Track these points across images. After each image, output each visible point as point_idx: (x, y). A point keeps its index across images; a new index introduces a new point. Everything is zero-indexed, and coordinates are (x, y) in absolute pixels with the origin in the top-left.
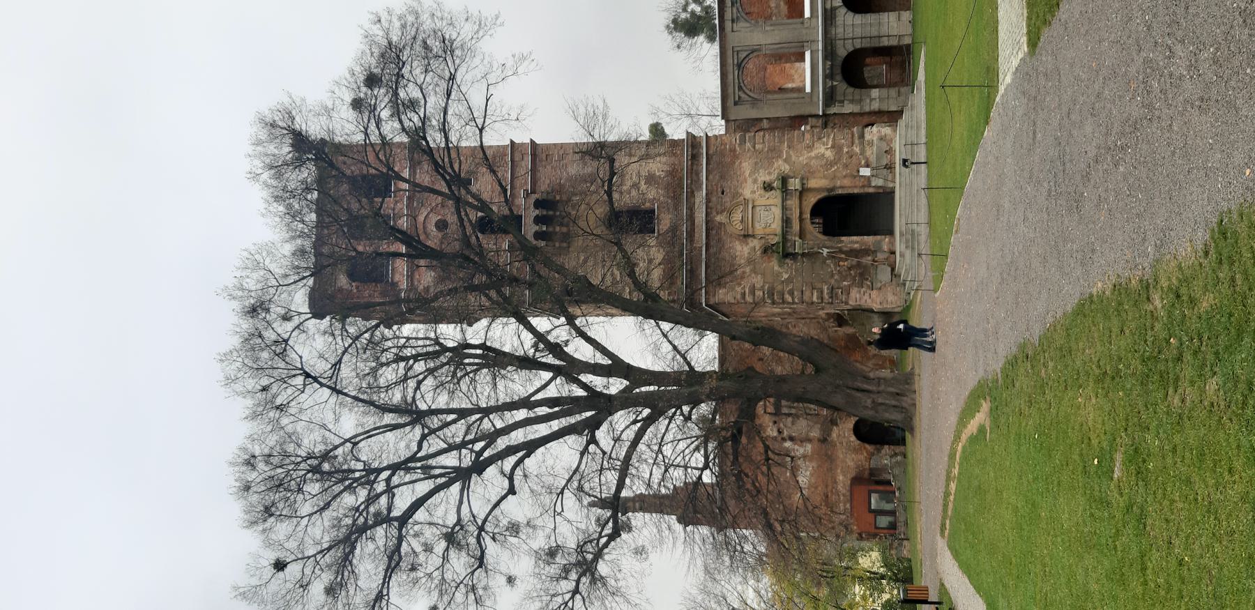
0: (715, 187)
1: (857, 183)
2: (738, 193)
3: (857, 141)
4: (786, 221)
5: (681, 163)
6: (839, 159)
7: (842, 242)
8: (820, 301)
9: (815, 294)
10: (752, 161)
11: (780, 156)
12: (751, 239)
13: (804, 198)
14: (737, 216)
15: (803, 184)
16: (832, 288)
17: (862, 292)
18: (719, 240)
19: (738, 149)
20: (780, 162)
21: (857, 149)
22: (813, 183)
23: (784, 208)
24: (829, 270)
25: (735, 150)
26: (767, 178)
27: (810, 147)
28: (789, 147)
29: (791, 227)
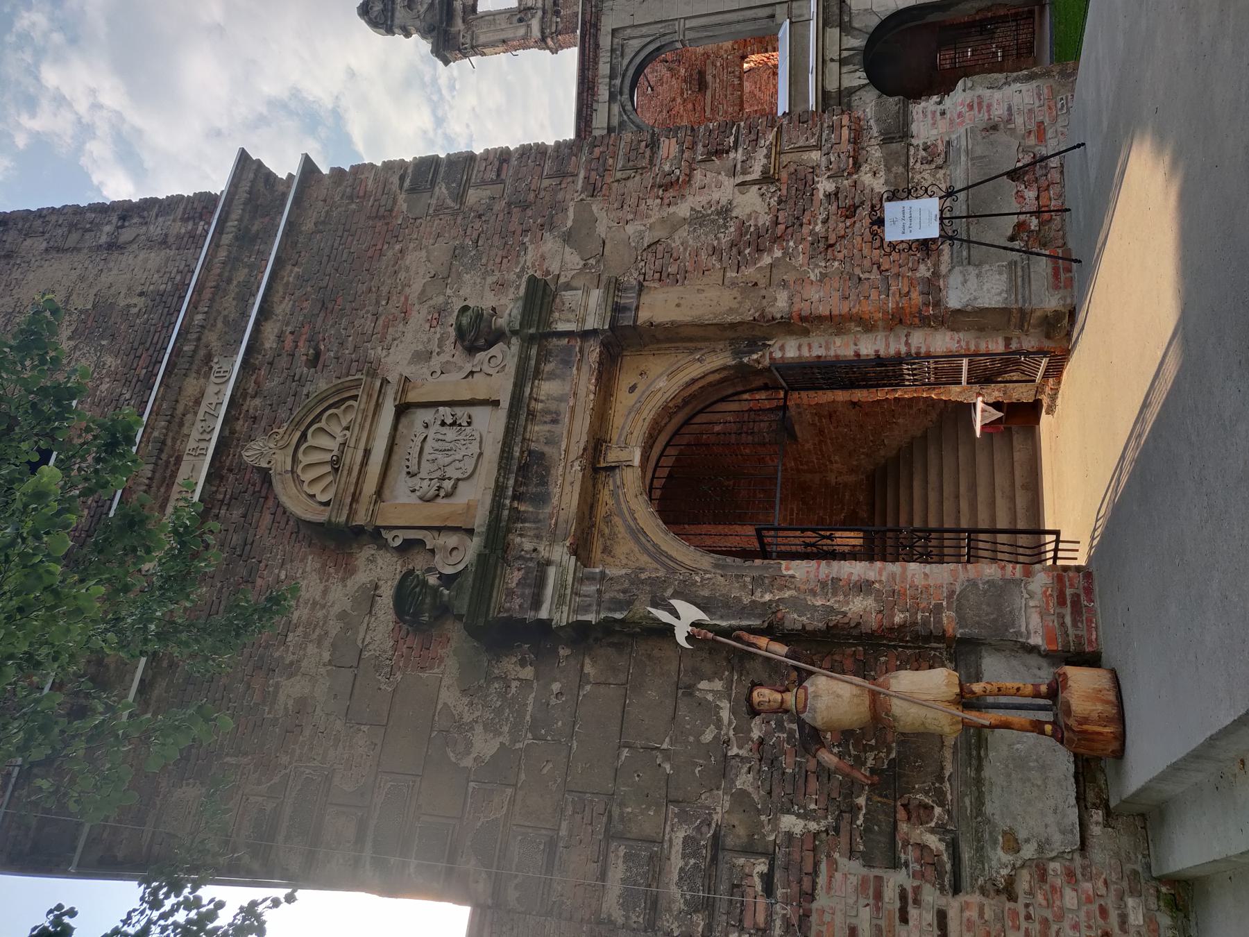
3: (875, 152)
4: (523, 469)
6: (798, 222)
7: (779, 582)
8: (638, 918)
9: (617, 872)
12: (369, 551)
13: (625, 380)
16: (716, 841)
17: (890, 895)
19: (402, 205)
24: (708, 737)
27: (672, 186)
28: (593, 190)
29: (541, 499)
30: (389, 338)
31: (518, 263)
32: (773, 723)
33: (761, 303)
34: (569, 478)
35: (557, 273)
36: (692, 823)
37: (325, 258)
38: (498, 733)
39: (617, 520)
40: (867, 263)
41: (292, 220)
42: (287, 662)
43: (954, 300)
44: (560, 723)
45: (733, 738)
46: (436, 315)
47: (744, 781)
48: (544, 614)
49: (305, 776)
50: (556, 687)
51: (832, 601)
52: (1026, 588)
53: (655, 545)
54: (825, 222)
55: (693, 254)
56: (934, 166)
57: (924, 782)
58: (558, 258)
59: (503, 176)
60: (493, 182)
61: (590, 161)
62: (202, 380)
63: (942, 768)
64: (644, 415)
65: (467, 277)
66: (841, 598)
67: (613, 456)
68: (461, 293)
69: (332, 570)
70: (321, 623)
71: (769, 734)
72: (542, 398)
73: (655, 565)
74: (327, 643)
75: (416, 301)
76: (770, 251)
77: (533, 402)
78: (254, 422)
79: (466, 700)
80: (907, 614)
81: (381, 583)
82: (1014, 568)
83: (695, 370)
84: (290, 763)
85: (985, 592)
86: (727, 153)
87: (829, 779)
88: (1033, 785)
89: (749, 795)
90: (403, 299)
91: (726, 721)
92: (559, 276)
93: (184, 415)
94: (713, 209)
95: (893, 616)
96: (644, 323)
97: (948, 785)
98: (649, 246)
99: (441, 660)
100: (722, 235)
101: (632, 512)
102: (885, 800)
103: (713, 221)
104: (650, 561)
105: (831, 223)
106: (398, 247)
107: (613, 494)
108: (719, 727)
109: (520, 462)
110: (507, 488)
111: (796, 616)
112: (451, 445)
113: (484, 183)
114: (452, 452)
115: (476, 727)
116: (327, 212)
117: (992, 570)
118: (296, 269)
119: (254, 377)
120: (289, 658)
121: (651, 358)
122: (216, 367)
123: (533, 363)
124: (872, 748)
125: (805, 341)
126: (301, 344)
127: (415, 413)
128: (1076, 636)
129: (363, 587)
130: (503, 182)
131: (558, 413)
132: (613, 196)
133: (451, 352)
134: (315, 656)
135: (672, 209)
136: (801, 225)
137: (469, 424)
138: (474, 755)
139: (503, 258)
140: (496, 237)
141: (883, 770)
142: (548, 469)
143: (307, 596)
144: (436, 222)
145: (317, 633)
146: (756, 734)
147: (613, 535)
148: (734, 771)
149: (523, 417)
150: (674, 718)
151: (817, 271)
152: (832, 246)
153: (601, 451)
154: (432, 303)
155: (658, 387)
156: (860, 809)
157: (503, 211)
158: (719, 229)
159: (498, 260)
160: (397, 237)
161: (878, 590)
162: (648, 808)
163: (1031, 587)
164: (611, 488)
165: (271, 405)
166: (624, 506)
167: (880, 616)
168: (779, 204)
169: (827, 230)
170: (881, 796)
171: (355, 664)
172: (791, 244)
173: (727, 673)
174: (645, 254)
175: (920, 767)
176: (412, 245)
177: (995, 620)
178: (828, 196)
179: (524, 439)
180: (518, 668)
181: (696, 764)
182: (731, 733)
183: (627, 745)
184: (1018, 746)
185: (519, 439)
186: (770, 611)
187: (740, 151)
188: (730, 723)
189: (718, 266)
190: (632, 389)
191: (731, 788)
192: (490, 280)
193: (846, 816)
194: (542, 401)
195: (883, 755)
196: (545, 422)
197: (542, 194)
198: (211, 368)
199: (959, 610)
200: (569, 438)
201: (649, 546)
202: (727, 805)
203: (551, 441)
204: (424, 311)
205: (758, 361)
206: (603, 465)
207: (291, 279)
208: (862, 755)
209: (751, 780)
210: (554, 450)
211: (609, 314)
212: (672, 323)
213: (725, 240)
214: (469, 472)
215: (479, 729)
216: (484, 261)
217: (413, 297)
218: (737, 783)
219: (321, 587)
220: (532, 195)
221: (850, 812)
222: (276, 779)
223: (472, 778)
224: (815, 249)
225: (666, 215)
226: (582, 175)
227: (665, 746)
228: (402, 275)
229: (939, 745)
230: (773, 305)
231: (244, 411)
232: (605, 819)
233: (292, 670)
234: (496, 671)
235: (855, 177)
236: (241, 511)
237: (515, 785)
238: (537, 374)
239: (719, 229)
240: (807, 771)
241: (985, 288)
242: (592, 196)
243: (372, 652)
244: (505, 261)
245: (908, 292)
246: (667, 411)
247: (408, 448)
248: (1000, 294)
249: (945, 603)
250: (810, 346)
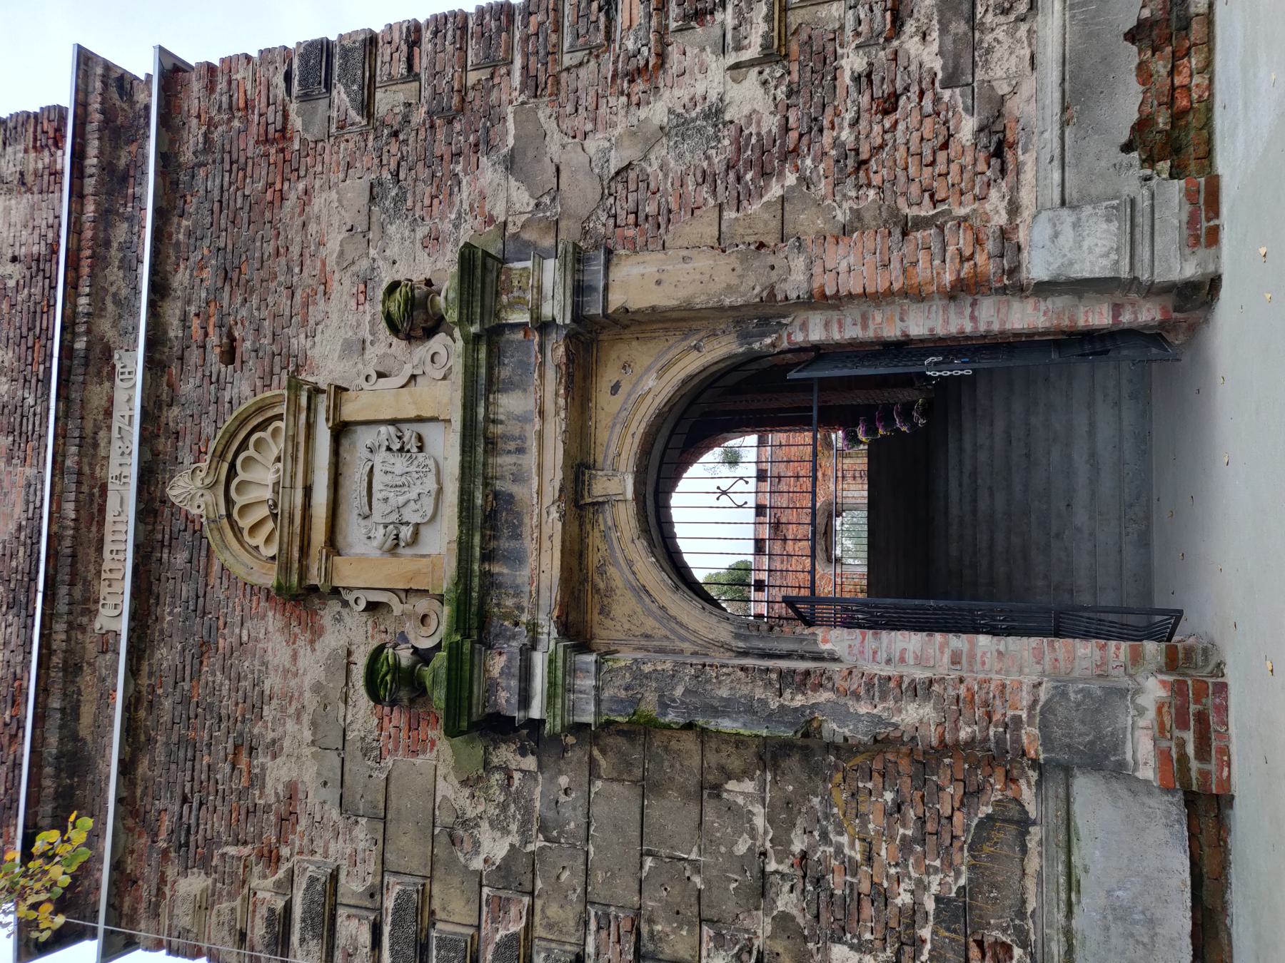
0: (196, 331)
1: (923, 271)
6: (815, 126)
11: (485, 144)
12: (334, 606)
15: (580, 290)
18: (199, 607)
20: (489, 173)
24: (742, 848)
28: (533, 85)
29: (516, 559)
30: (312, 322)
31: (451, 204)
32: (816, 834)
33: (769, 277)
34: (547, 531)
35: (502, 219)
36: (731, 949)
37: (216, 205)
38: (505, 831)
39: (611, 570)
40: (914, 189)
41: (165, 149)
42: (268, 740)
43: (1037, 268)
44: (572, 825)
45: (771, 852)
46: (362, 287)
47: (786, 901)
48: (536, 712)
49: (308, 874)
50: (564, 781)
51: (880, 707)
52: (1133, 701)
53: (662, 608)
54: (855, 123)
55: (677, 184)
56: (1012, 17)
57: (1001, 917)
58: (502, 195)
59: (416, 69)
60: (404, 80)
61: (526, 39)
62: (107, 384)
63: (1024, 902)
64: (633, 428)
65: (392, 229)
66: (891, 704)
67: (601, 487)
68: (388, 253)
69: (297, 630)
70: (296, 694)
71: (814, 847)
72: (502, 417)
73: (664, 632)
74: (306, 719)
75: (335, 268)
76: (781, 174)
77: (491, 426)
78: (177, 438)
79: (467, 792)
80: (976, 728)
81: (353, 647)
82: (1118, 649)
83: (692, 364)
84: (291, 855)
85: (1078, 705)
86: (712, 13)
87: (886, 905)
88: (1137, 942)
89: (793, 918)
90: (319, 264)
91: (761, 830)
92: (505, 224)
93: (96, 433)
94: (698, 109)
95: (957, 730)
96: (617, 310)
97: (1030, 922)
98: (617, 173)
99: (433, 744)
100: (713, 152)
101: (630, 563)
102: (954, 935)
103: (699, 130)
104: (657, 625)
105: (863, 124)
106: (301, 186)
107: (605, 536)
108: (753, 838)
109: (484, 510)
110: (472, 547)
111: (835, 727)
112: (403, 479)
113: (392, 80)
114: (406, 489)
115: (482, 823)
116: (205, 135)
117: (1088, 651)
118: (185, 223)
119: (165, 378)
120: (270, 736)
121: (635, 343)
122: (118, 366)
123: (483, 371)
124: (936, 870)
125: (834, 315)
126: (210, 330)
127: (355, 432)
128: (1201, 772)
129: (333, 654)
130: (417, 77)
131: (522, 438)
132: (563, 94)
133: (386, 346)
134: (297, 733)
135: (643, 113)
136: (821, 130)
137: (421, 449)
138: (482, 857)
139: (432, 197)
140: (421, 164)
141: (949, 900)
142: (519, 515)
143: (276, 661)
144: (342, 146)
145: (294, 707)
146: (797, 847)
147: (610, 591)
148: (774, 889)
149: (480, 450)
150: (701, 823)
151: (846, 205)
152: (866, 162)
153: (583, 482)
154: (354, 268)
155: (646, 388)
156: (924, 941)
157: (424, 124)
158: (708, 143)
159: (427, 202)
160: (297, 170)
161: (939, 695)
162: (680, 927)
163: (1141, 700)
164: (602, 528)
165: (192, 416)
166: (619, 555)
167: (940, 729)
168: (788, 97)
169: (857, 139)
170: (948, 929)
171: (340, 747)
172: (808, 162)
173: (758, 772)
174: (613, 184)
175: (996, 899)
176: (318, 183)
177: (1092, 743)
178: (857, 79)
179: (485, 478)
180: (518, 758)
181: (730, 880)
182: (768, 845)
183: (649, 853)
184: (1120, 893)
185: (479, 481)
186: (803, 720)
187: (730, 9)
188: (766, 832)
189: (711, 202)
190: (615, 389)
191: (772, 909)
192: (421, 232)
193: (907, 948)
194: (501, 422)
195: (950, 880)
196: (509, 452)
197: (471, 94)
198: (114, 367)
199: (1044, 727)
200: (540, 474)
201: (654, 607)
202: (769, 928)
203: (518, 478)
204: (347, 282)
205: (773, 345)
206: (589, 500)
207: (181, 237)
208: (925, 878)
209: (795, 901)
210: (525, 490)
211: (569, 301)
212: (653, 308)
213: (718, 161)
214: (430, 513)
215: (485, 825)
216: (410, 203)
217: (332, 262)
218: (779, 903)
219: (289, 652)
220: (456, 100)
221: (913, 944)
222: (281, 874)
223: (484, 882)
224: (841, 170)
225: (636, 123)
226: (518, 62)
227: (693, 856)
228: (312, 228)
229: (1019, 873)
230: (785, 280)
231: (163, 425)
232: (633, 938)
233: (275, 749)
234: (496, 760)
235: (895, 43)
236: (186, 555)
237: (532, 893)
238: (493, 385)
239: (708, 143)
240: (859, 894)
241: (1086, 244)
242: (536, 96)
243: (356, 733)
244: (436, 201)
245: (973, 254)
246: (661, 417)
248: (1107, 255)
249: (1024, 716)
250: (841, 325)
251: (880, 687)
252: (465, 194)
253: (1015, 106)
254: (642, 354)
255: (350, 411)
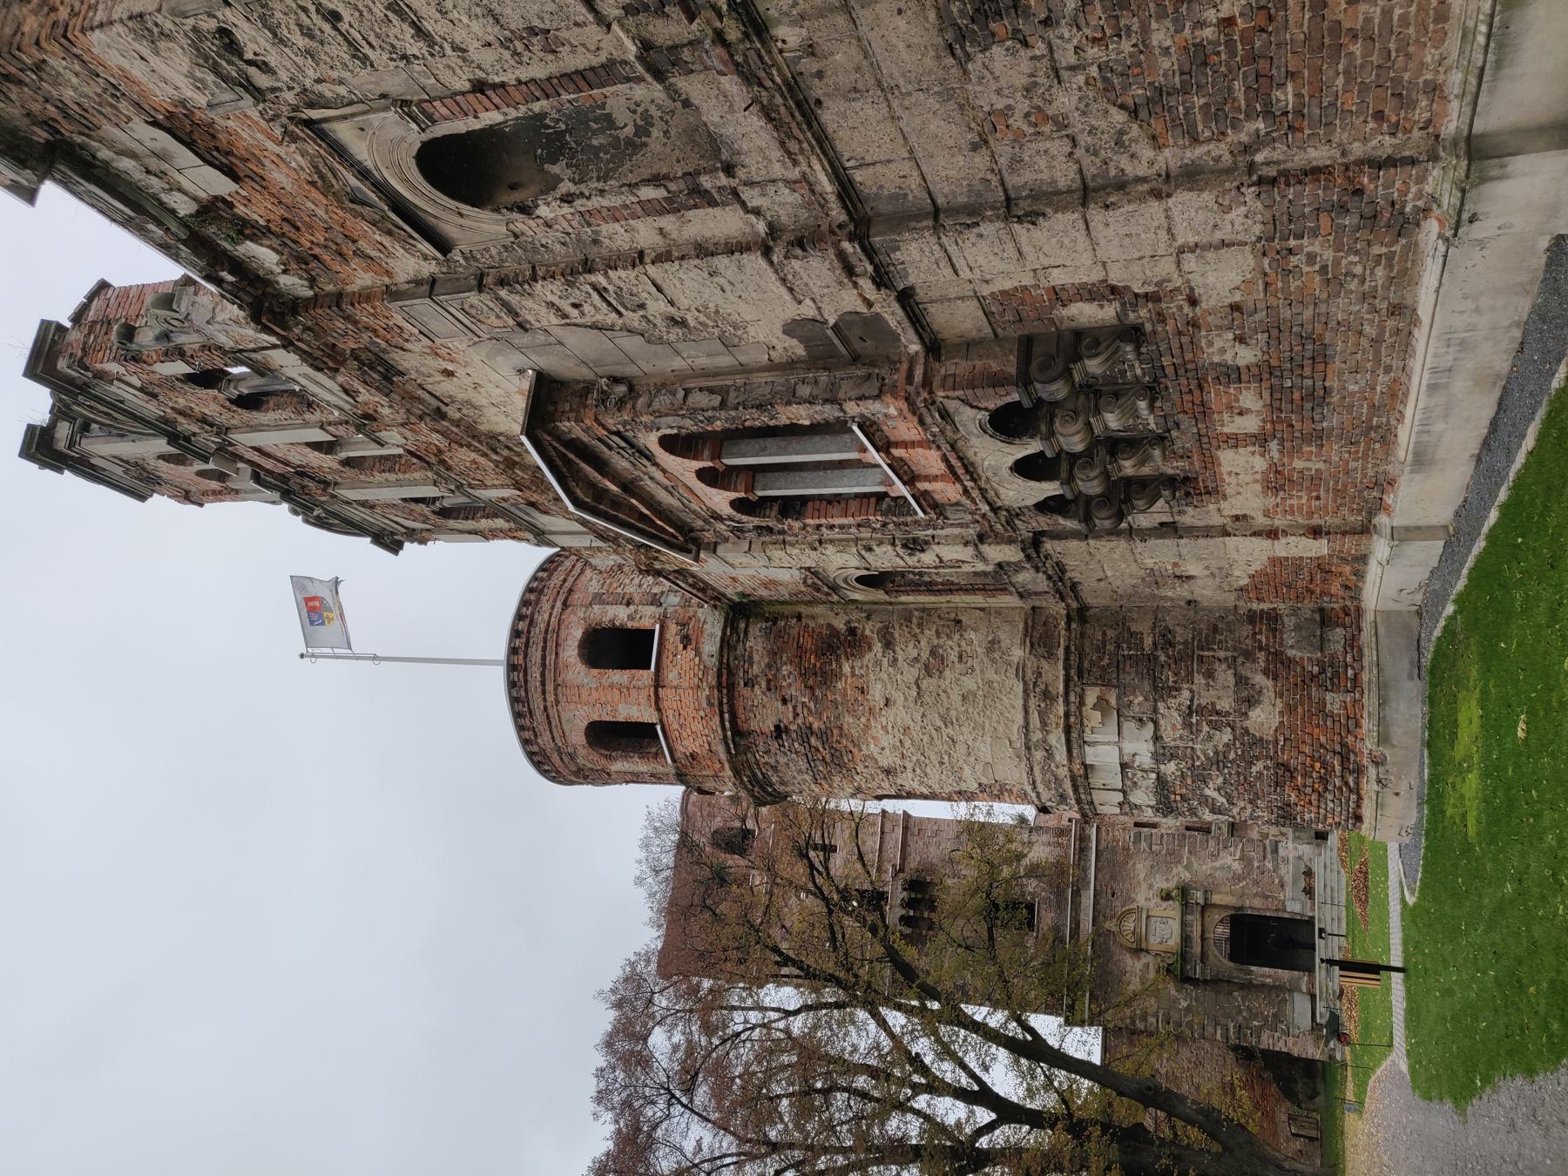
2: (1130, 898)
3: (1269, 856)
5: (1067, 856)
7: (1251, 972)
9: (1219, 1032)
10: (1148, 863)
11: (1179, 862)
14: (1129, 925)
15: (1206, 899)
20: (1180, 868)
21: (1270, 866)
22: (1216, 899)
23: (1183, 924)
25: (1128, 849)
26: (1165, 885)
27: (1215, 856)
28: (1190, 852)
247: (1152, 927)
251: (1263, 976)
252: (1174, 871)
253: (1286, 879)
254: (1215, 911)
255: (1151, 913)
